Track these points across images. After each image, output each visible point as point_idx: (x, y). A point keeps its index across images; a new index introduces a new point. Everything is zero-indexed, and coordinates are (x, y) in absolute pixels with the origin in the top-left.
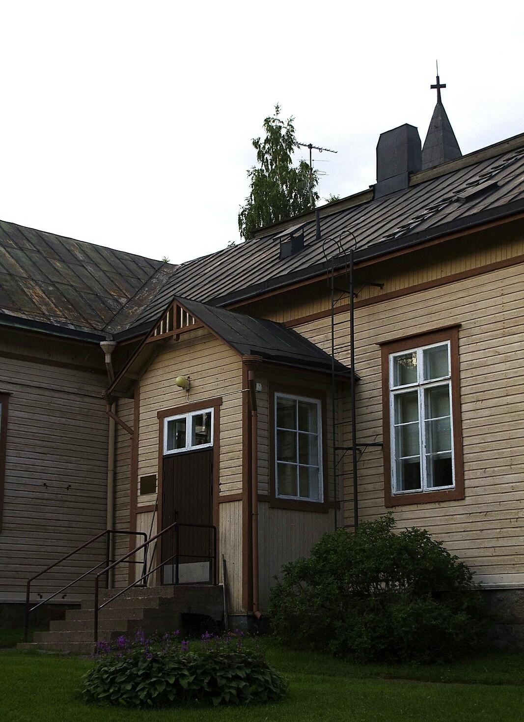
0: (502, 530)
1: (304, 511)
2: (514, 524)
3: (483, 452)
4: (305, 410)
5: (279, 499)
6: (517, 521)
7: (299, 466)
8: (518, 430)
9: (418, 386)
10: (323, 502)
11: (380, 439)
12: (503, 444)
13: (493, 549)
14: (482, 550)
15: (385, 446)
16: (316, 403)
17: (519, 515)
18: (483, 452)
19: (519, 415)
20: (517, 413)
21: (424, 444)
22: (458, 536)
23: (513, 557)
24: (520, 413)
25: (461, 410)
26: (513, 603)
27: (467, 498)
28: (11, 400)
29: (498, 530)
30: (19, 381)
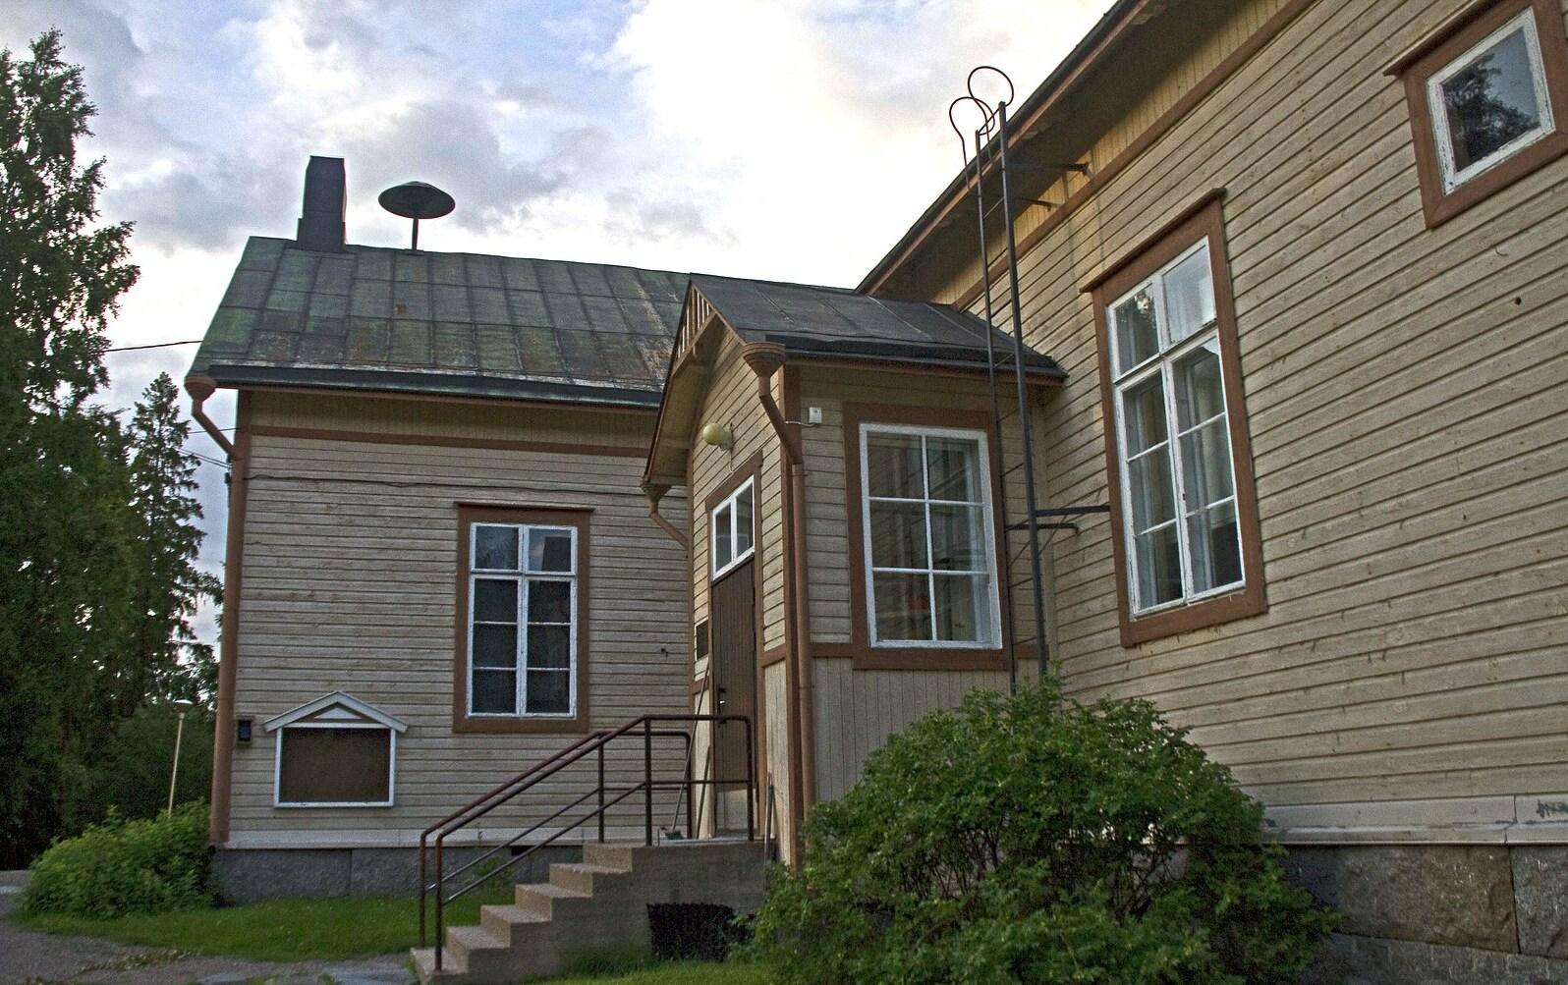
0: (1351, 685)
1: (949, 670)
2: (1378, 666)
3: (1297, 486)
4: (952, 461)
5: (881, 650)
6: (1384, 658)
7: (934, 575)
8: (1369, 413)
9: (1161, 358)
10: (1001, 647)
11: (1104, 498)
12: (1340, 456)
13: (1335, 736)
14: (1310, 740)
15: (1113, 508)
16: (975, 438)
17: (1388, 641)
18: (1297, 486)
19: (1367, 370)
20: (1363, 367)
21: (1182, 491)
22: (1258, 707)
23: (1378, 756)
24: (1369, 364)
25: (1244, 392)
26: (1385, 883)
27: (1272, 610)
28: (593, 520)
29: (1343, 687)
30: (609, 488)
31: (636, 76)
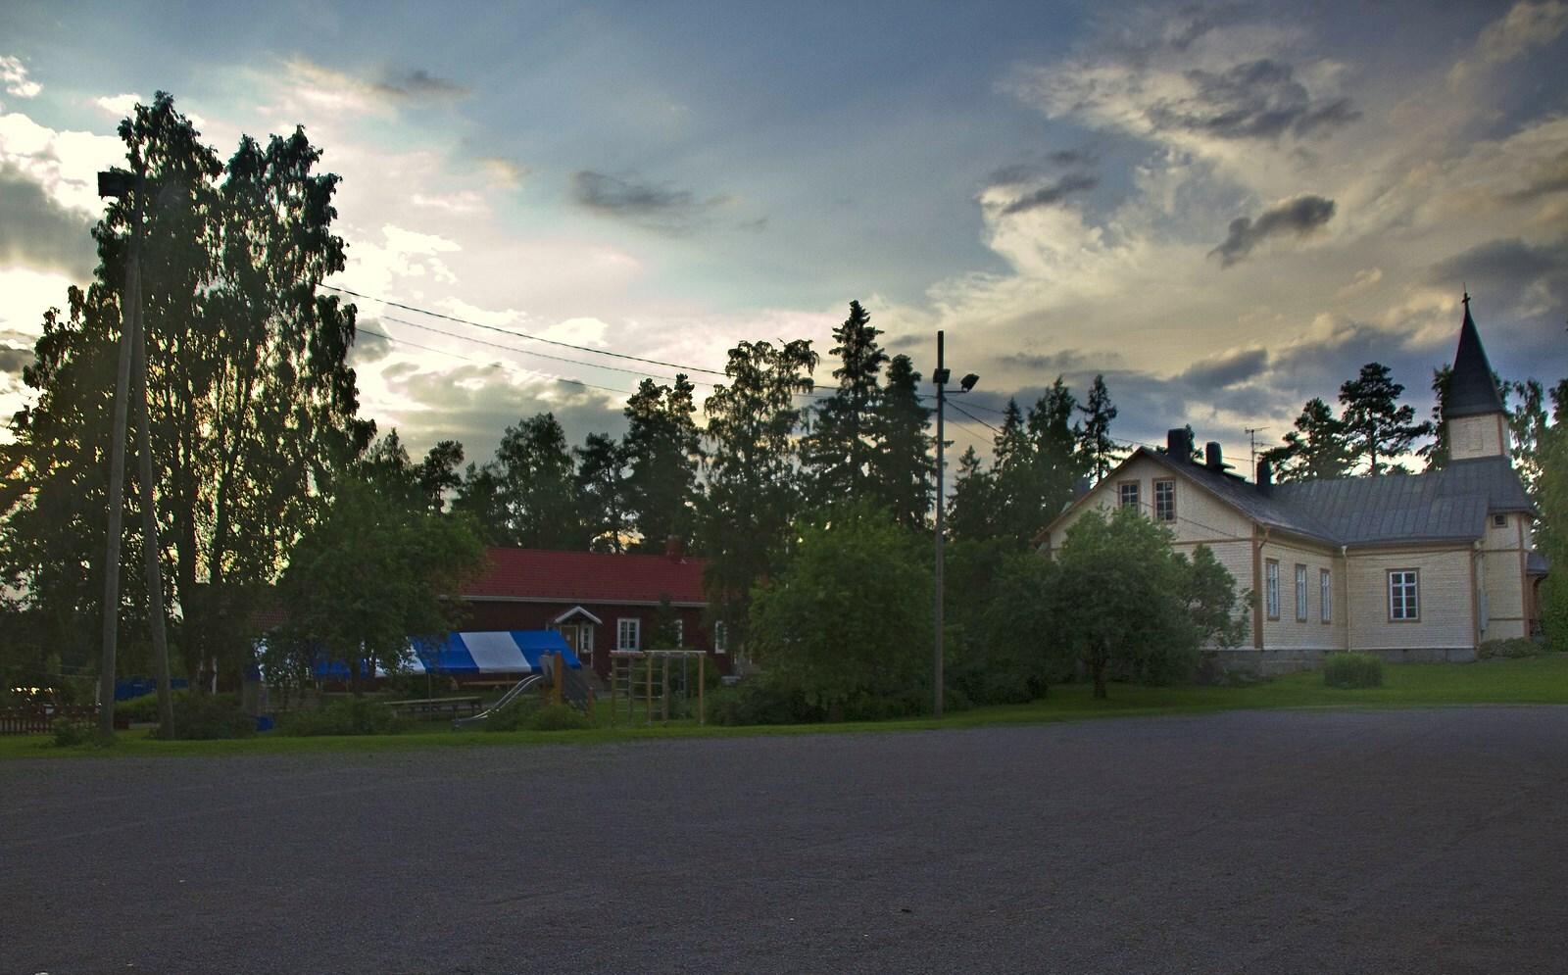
31: (1007, 411)
